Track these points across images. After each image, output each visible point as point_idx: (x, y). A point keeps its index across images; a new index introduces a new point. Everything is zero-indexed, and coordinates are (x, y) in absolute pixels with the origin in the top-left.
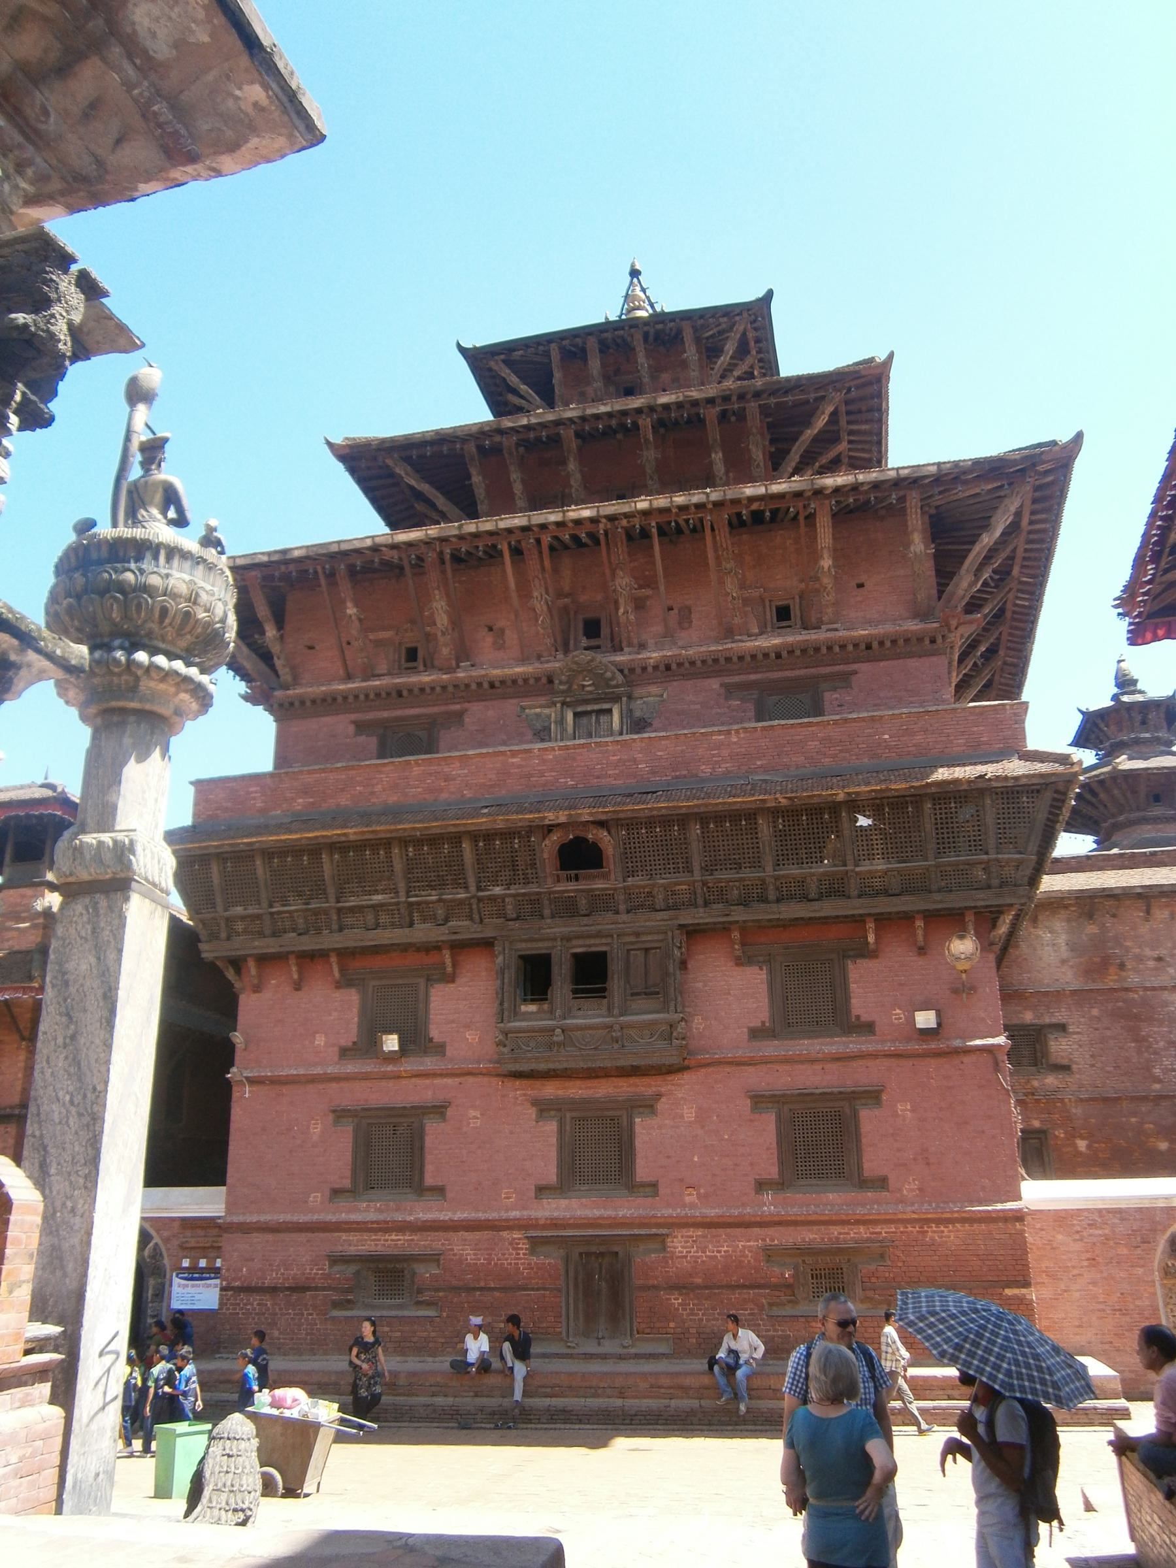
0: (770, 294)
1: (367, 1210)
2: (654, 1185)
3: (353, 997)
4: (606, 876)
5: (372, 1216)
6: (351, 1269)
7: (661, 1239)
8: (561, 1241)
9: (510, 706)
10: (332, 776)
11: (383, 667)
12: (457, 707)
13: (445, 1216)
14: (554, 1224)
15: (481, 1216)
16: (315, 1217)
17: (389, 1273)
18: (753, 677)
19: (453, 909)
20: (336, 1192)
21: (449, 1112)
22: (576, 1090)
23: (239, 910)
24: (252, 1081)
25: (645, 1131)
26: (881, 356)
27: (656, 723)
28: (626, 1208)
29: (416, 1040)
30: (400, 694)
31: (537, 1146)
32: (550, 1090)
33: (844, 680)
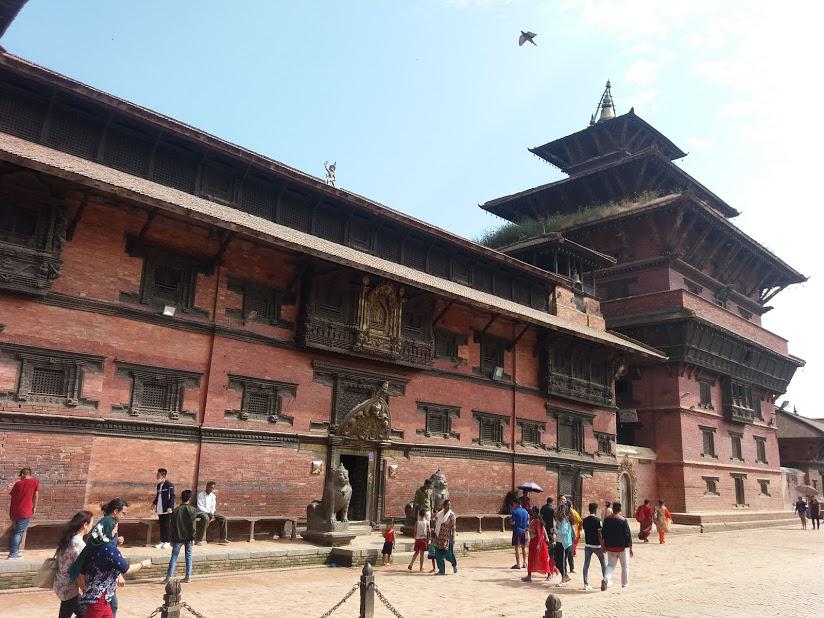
3: (697, 385)
7: (745, 476)
24: (690, 412)
32: (734, 429)
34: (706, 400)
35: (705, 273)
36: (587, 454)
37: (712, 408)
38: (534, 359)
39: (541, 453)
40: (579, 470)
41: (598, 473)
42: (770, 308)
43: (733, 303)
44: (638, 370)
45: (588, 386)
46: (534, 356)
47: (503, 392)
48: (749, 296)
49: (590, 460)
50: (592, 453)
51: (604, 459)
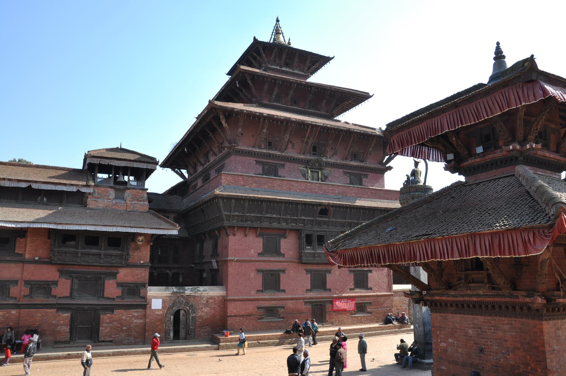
0: (333, 57)
1: (266, 295)
2: (330, 290)
3: (260, 240)
4: (329, 218)
5: (267, 297)
6: (262, 310)
7: (332, 302)
8: (311, 303)
9: (296, 166)
10: (263, 179)
11: (263, 147)
12: (283, 163)
13: (286, 297)
14: (310, 298)
15: (293, 297)
16: (254, 297)
17: (271, 311)
18: (349, 171)
19: (296, 221)
20: (258, 291)
21: (286, 271)
22: (315, 267)
23: (237, 213)
25: (329, 277)
26: (371, 94)
27: (330, 178)
28: (325, 294)
29: (277, 252)
30: (270, 156)
31: (306, 280)
33: (367, 176)
34: (272, 249)
35: (291, 153)
36: (108, 298)
37: (277, 252)
38: (49, 240)
39: (51, 301)
40: (97, 309)
41: (116, 312)
42: (390, 168)
43: (333, 170)
44: (216, 232)
45: (99, 255)
46: (49, 239)
47: (13, 265)
48: (362, 161)
49: (109, 303)
50: (114, 297)
51: (128, 301)
